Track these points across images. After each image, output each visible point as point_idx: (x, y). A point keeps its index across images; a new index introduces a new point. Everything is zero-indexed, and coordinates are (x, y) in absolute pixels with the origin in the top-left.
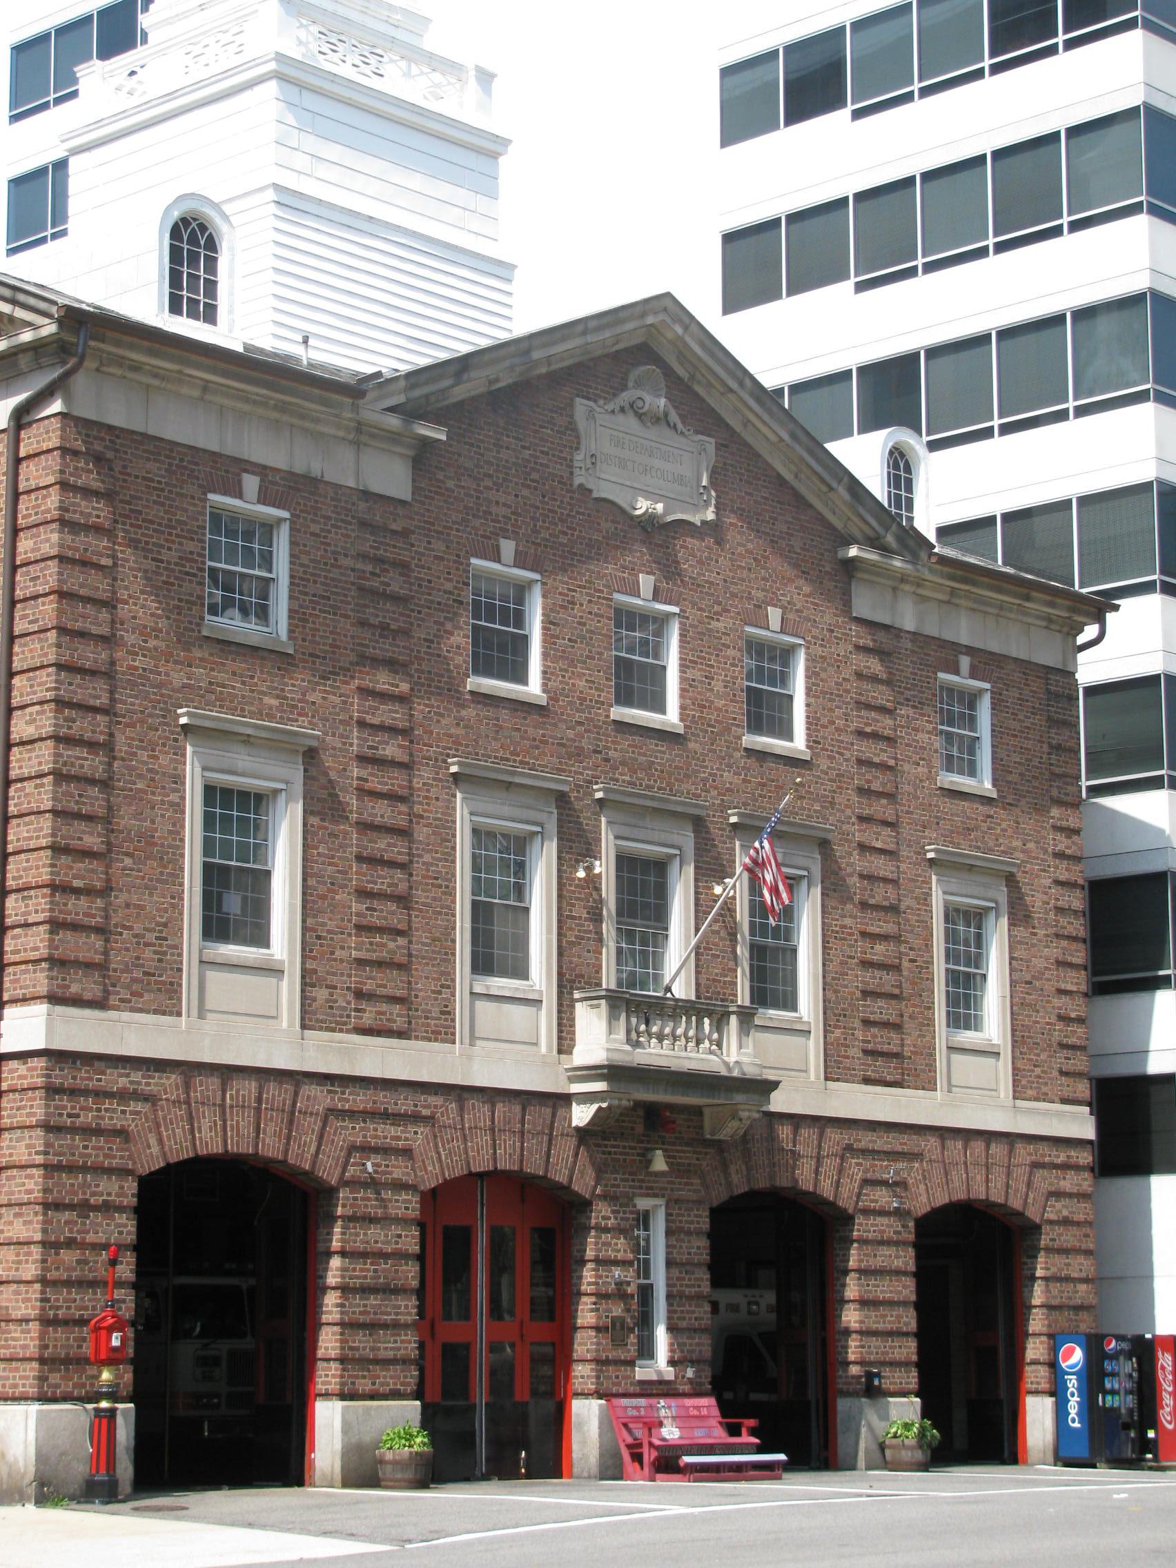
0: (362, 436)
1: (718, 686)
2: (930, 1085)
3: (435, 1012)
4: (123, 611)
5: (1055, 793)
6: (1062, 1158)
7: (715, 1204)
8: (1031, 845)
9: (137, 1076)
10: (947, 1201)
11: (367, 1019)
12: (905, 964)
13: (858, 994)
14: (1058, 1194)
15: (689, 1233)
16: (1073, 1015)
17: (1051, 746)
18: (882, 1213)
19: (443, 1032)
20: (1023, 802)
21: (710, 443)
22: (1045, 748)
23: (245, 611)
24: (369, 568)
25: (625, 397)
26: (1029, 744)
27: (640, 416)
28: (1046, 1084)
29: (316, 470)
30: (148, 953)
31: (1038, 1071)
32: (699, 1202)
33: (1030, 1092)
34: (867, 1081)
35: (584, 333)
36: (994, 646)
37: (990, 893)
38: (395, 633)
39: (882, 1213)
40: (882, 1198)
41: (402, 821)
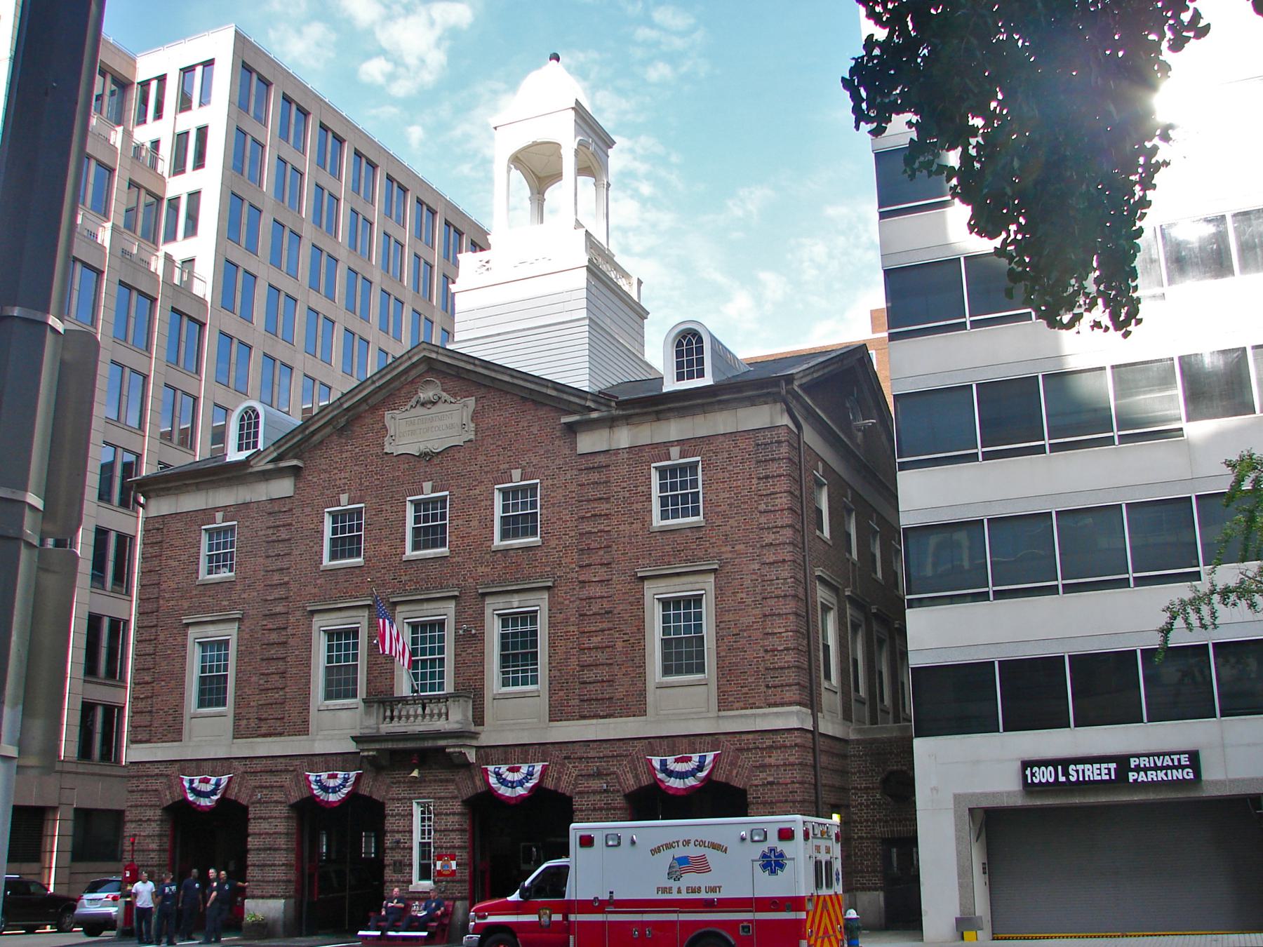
0: (266, 476)
1: (475, 523)
2: (644, 713)
3: (299, 722)
5: (762, 507)
6: (769, 743)
9: (162, 768)
11: (263, 731)
12: (619, 644)
14: (763, 767)
15: (446, 814)
18: (594, 792)
19: (304, 731)
20: (732, 522)
21: (471, 402)
22: (755, 481)
24: (271, 531)
25: (413, 402)
27: (423, 405)
29: (248, 500)
30: (170, 718)
31: (745, 690)
32: (455, 797)
33: (737, 705)
34: (583, 717)
35: (374, 382)
39: (594, 792)
40: (596, 784)
41: (283, 639)
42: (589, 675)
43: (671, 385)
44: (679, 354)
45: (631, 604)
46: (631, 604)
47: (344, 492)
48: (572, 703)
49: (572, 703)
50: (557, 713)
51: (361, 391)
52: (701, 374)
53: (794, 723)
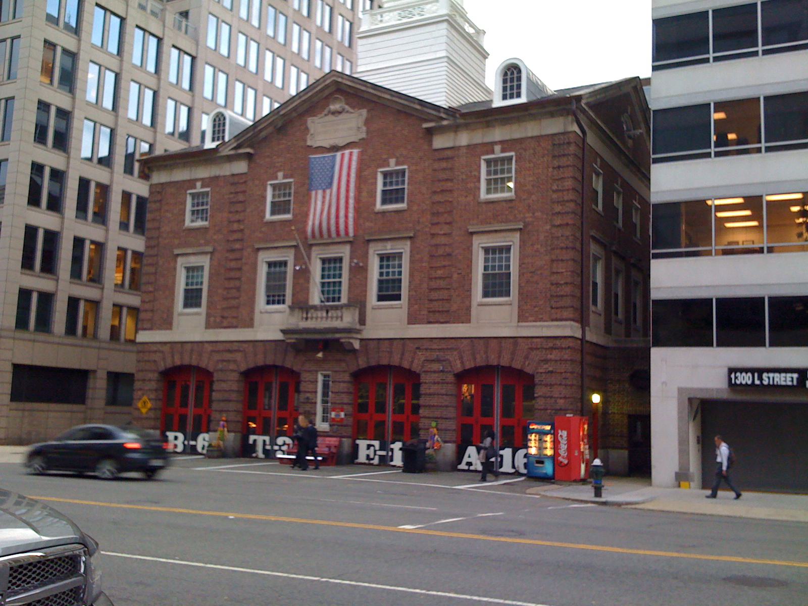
0: (230, 159)
2: (469, 321)
4: (163, 229)
5: (555, 187)
6: (550, 345)
7: (352, 372)
8: (536, 214)
10: (473, 366)
11: (225, 324)
12: (455, 276)
13: (427, 290)
14: (546, 361)
15: (340, 382)
16: (562, 282)
17: (554, 168)
18: (435, 372)
20: (533, 197)
22: (550, 170)
23: (202, 219)
24: (232, 196)
25: (326, 112)
26: (540, 171)
28: (542, 314)
31: (536, 309)
32: (344, 371)
33: (530, 319)
34: (430, 323)
35: (300, 97)
36: (517, 135)
37: (508, 239)
38: (240, 212)
39: (435, 372)
40: (436, 366)
42: (435, 295)
43: (498, 103)
44: (505, 81)
45: (464, 250)
46: (464, 250)
47: (280, 170)
48: (423, 313)
49: (423, 313)
50: (413, 319)
51: (292, 103)
52: (519, 95)
53: (567, 332)
